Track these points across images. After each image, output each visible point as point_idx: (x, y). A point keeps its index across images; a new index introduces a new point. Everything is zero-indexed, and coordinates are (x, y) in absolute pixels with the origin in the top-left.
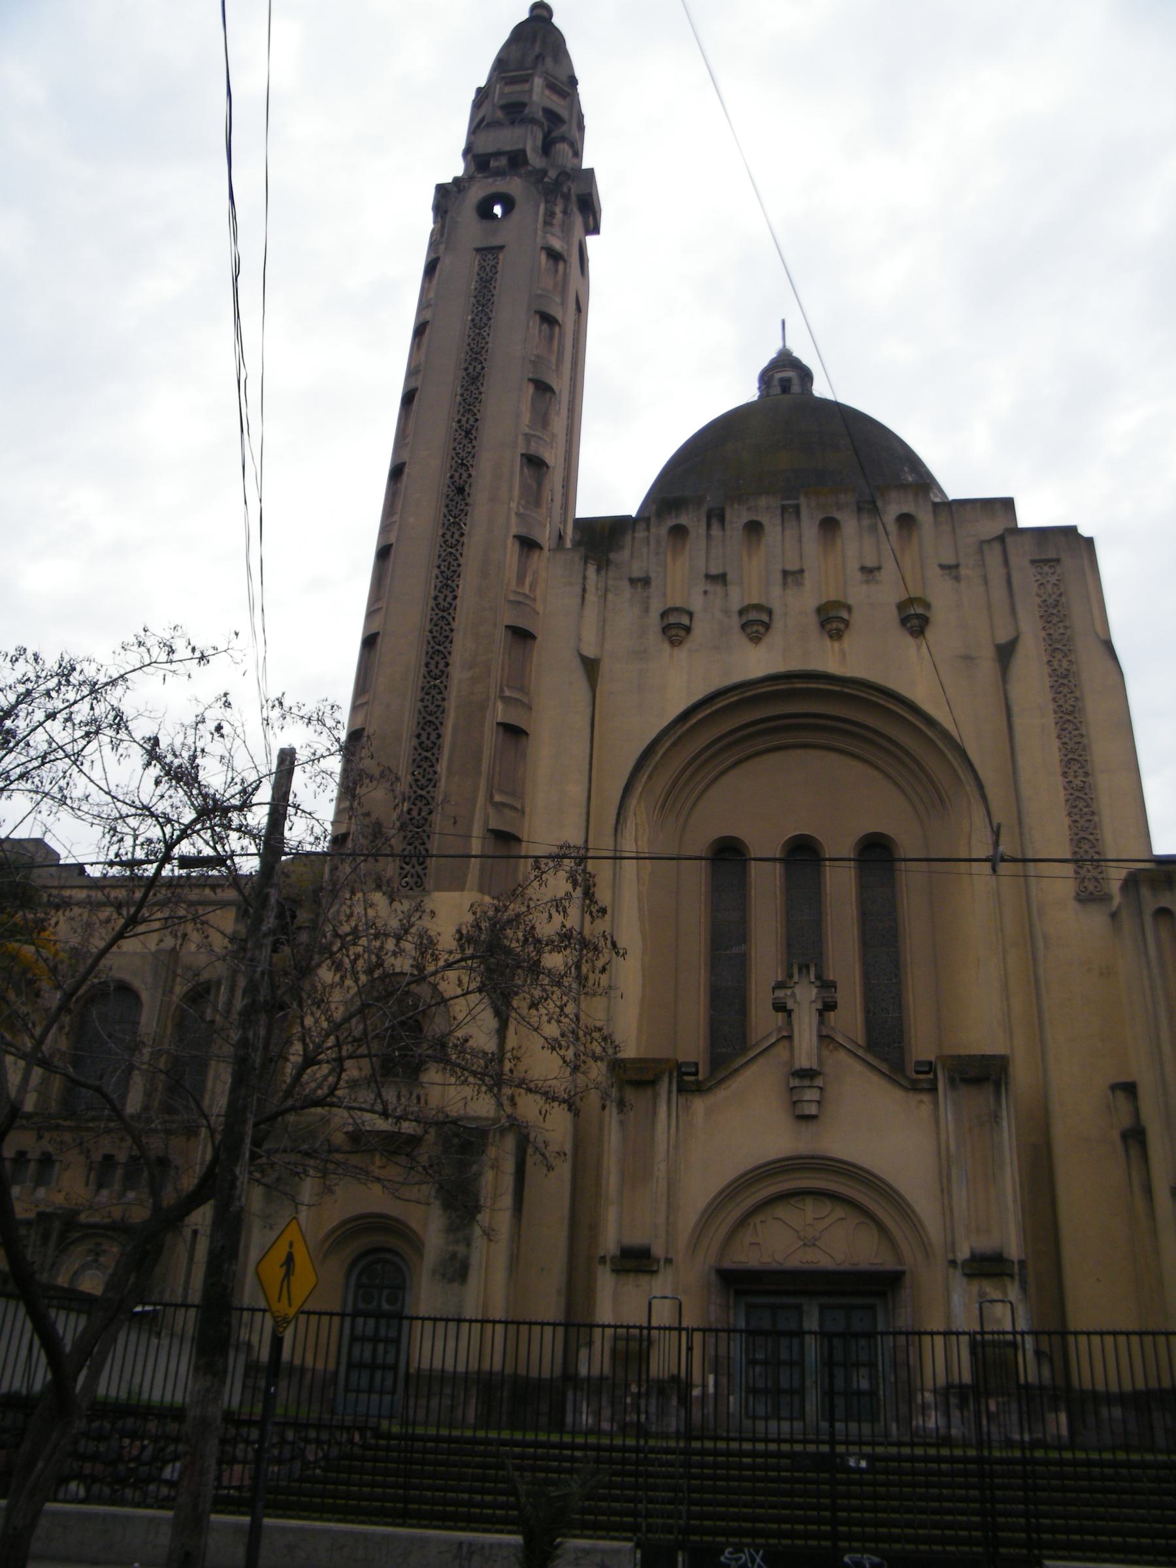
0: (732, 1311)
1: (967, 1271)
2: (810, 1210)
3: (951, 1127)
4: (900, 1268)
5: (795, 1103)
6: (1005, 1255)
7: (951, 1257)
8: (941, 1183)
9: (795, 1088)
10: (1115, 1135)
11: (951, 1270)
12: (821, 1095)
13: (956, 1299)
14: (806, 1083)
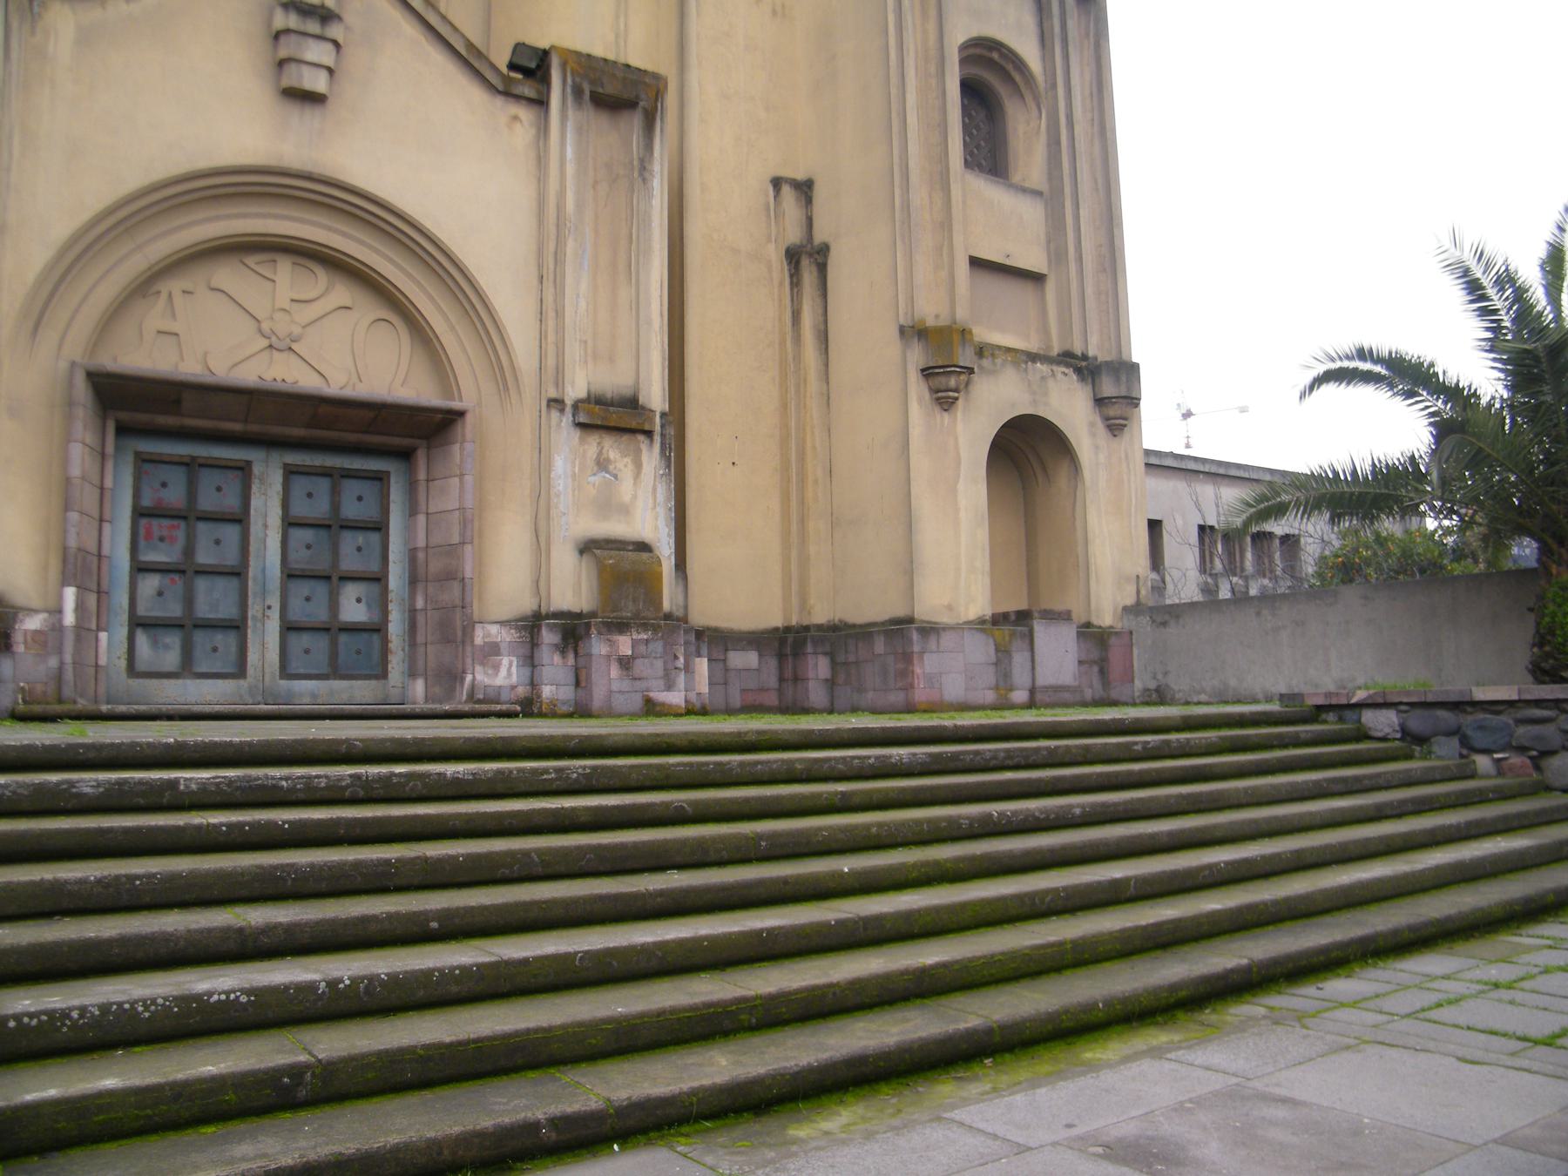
0: (110, 465)
1: (582, 419)
2: (286, 277)
3: (570, 169)
4: (456, 405)
5: (281, 63)
6: (641, 401)
7: (553, 394)
8: (540, 266)
9: (288, 31)
10: (775, 255)
11: (555, 414)
12: (338, 60)
13: (560, 465)
14: (313, 27)
